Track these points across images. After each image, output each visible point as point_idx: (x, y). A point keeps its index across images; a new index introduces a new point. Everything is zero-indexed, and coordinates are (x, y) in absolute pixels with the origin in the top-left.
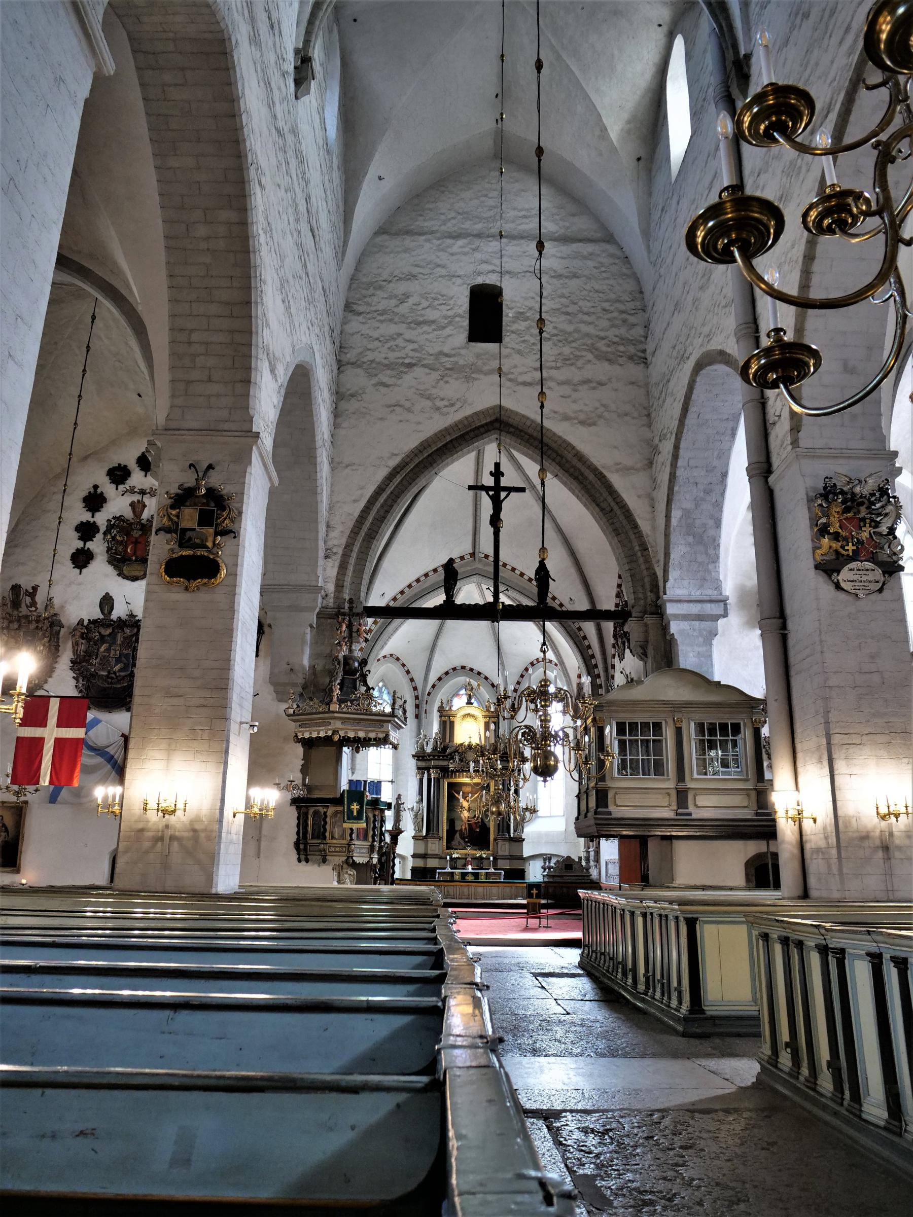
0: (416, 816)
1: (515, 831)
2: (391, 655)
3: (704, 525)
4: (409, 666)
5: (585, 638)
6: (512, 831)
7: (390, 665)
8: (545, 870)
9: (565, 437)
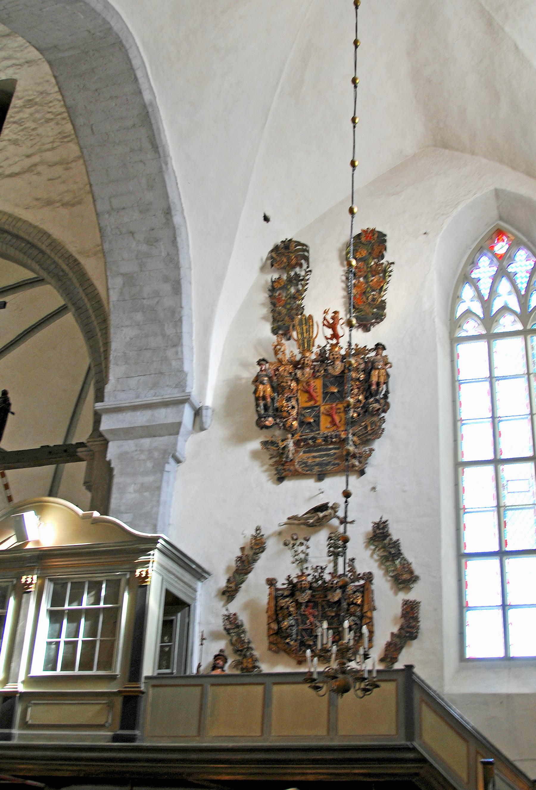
3: (157, 294)
9: (41, 226)
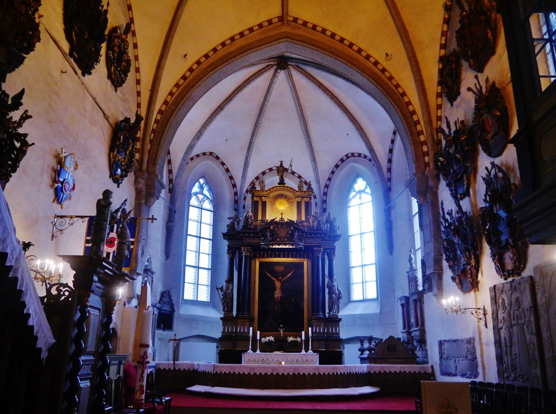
0: (225, 295)
1: (330, 310)
2: (211, 154)
4: (228, 165)
5: (404, 94)
6: (327, 310)
7: (209, 162)
8: (362, 354)
